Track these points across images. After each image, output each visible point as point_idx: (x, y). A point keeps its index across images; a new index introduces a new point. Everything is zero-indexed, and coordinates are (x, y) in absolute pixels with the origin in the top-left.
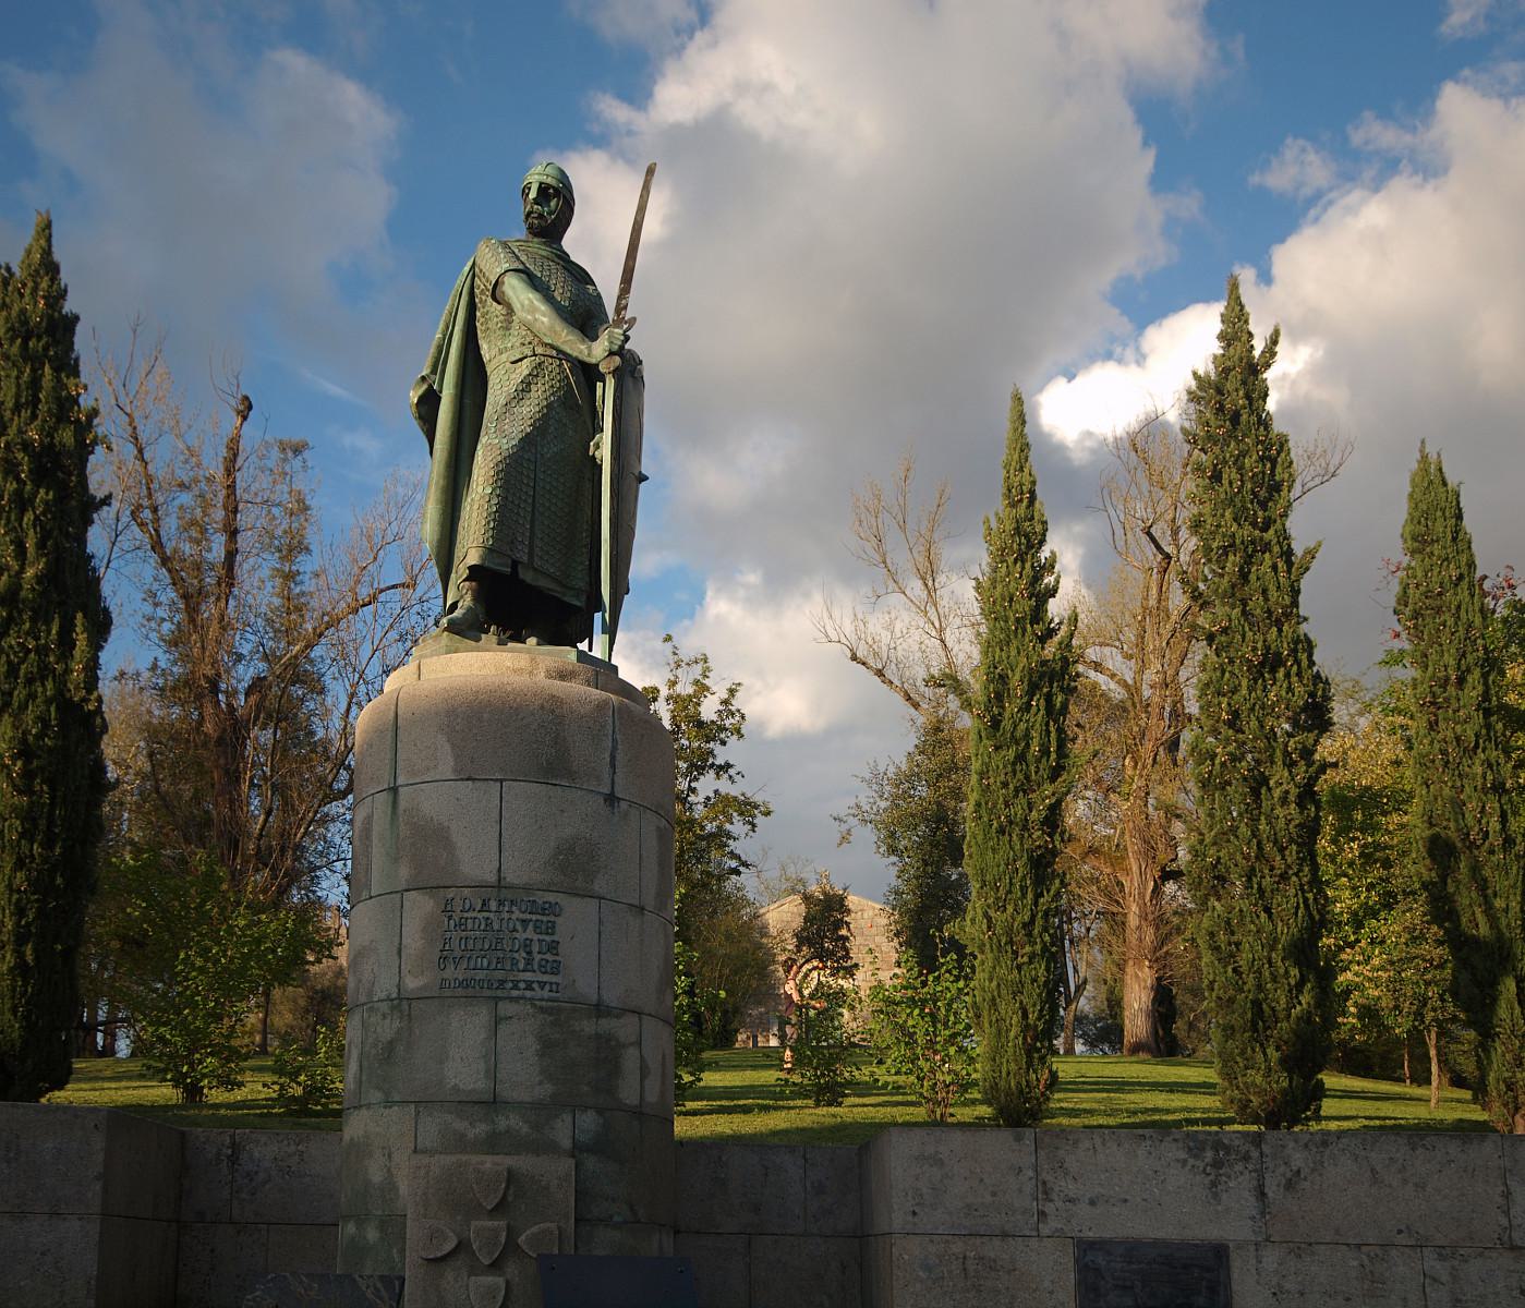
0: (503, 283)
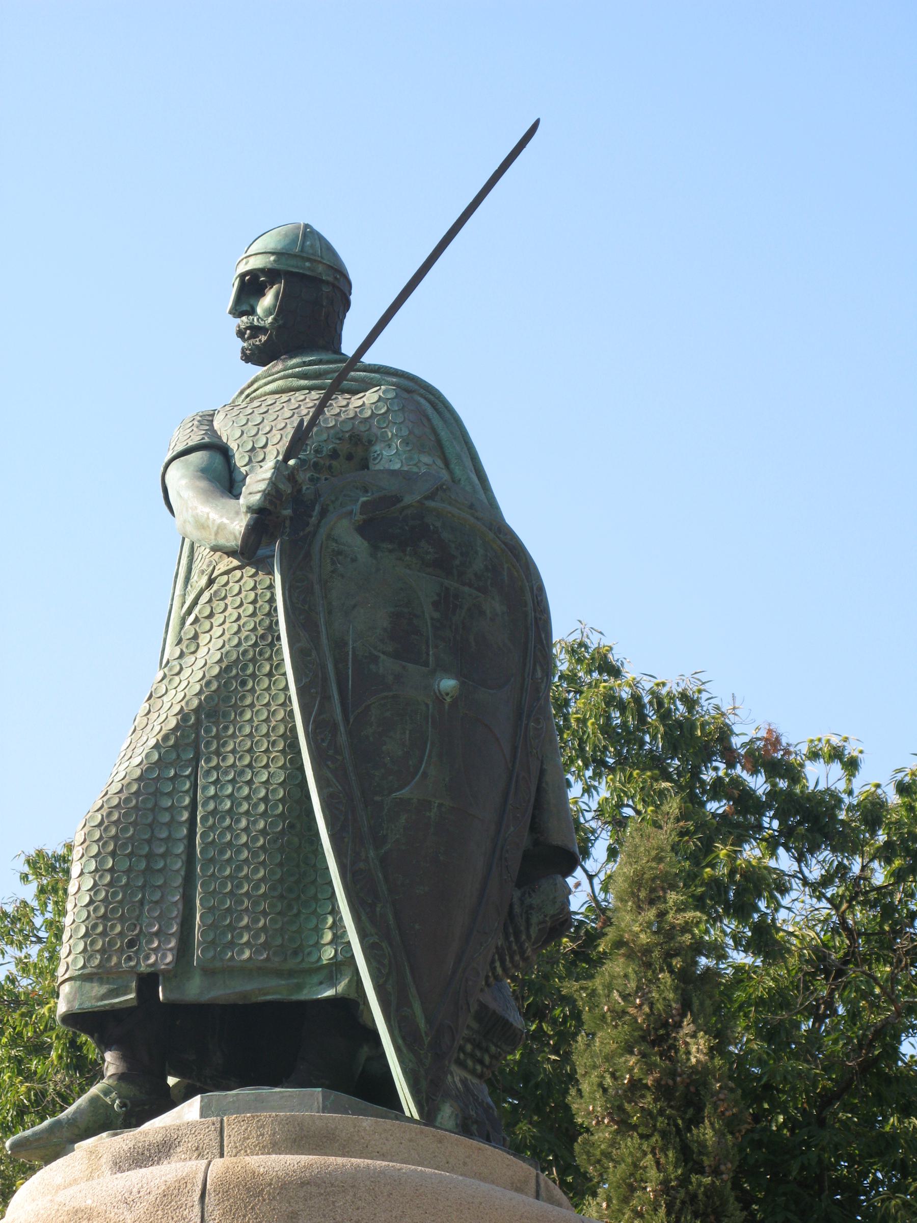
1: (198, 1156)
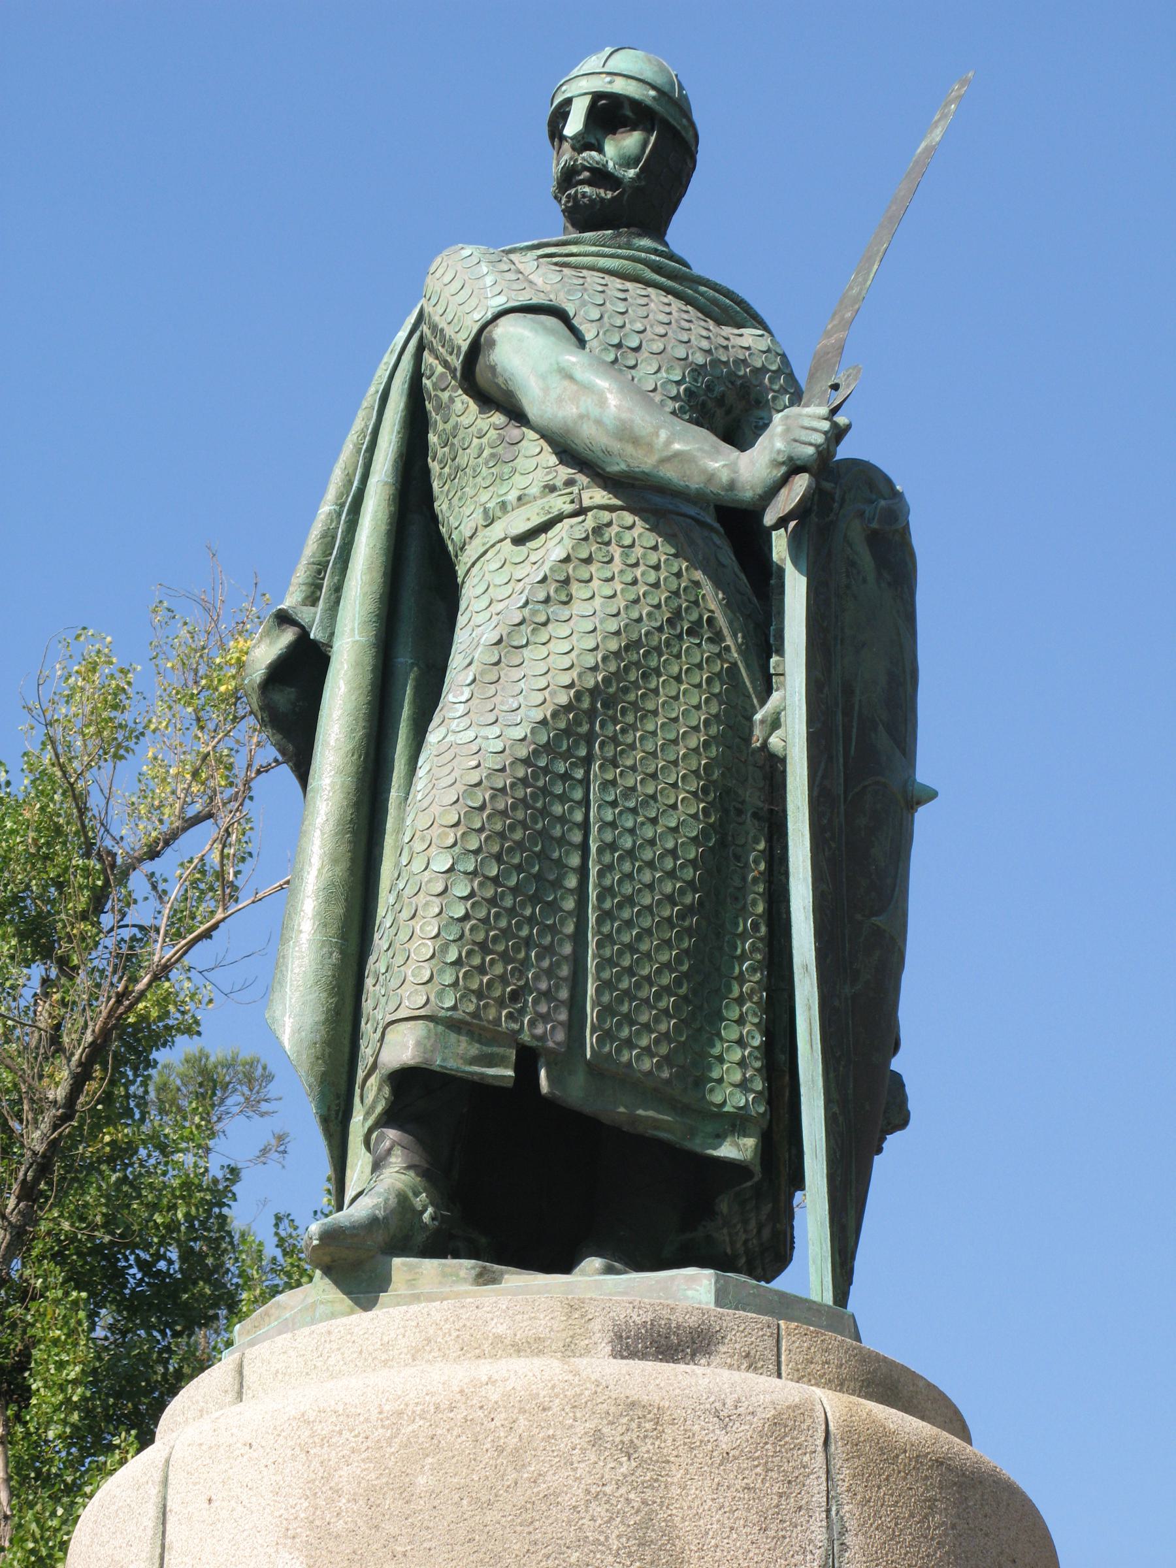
0: (492, 343)
1: (750, 1367)
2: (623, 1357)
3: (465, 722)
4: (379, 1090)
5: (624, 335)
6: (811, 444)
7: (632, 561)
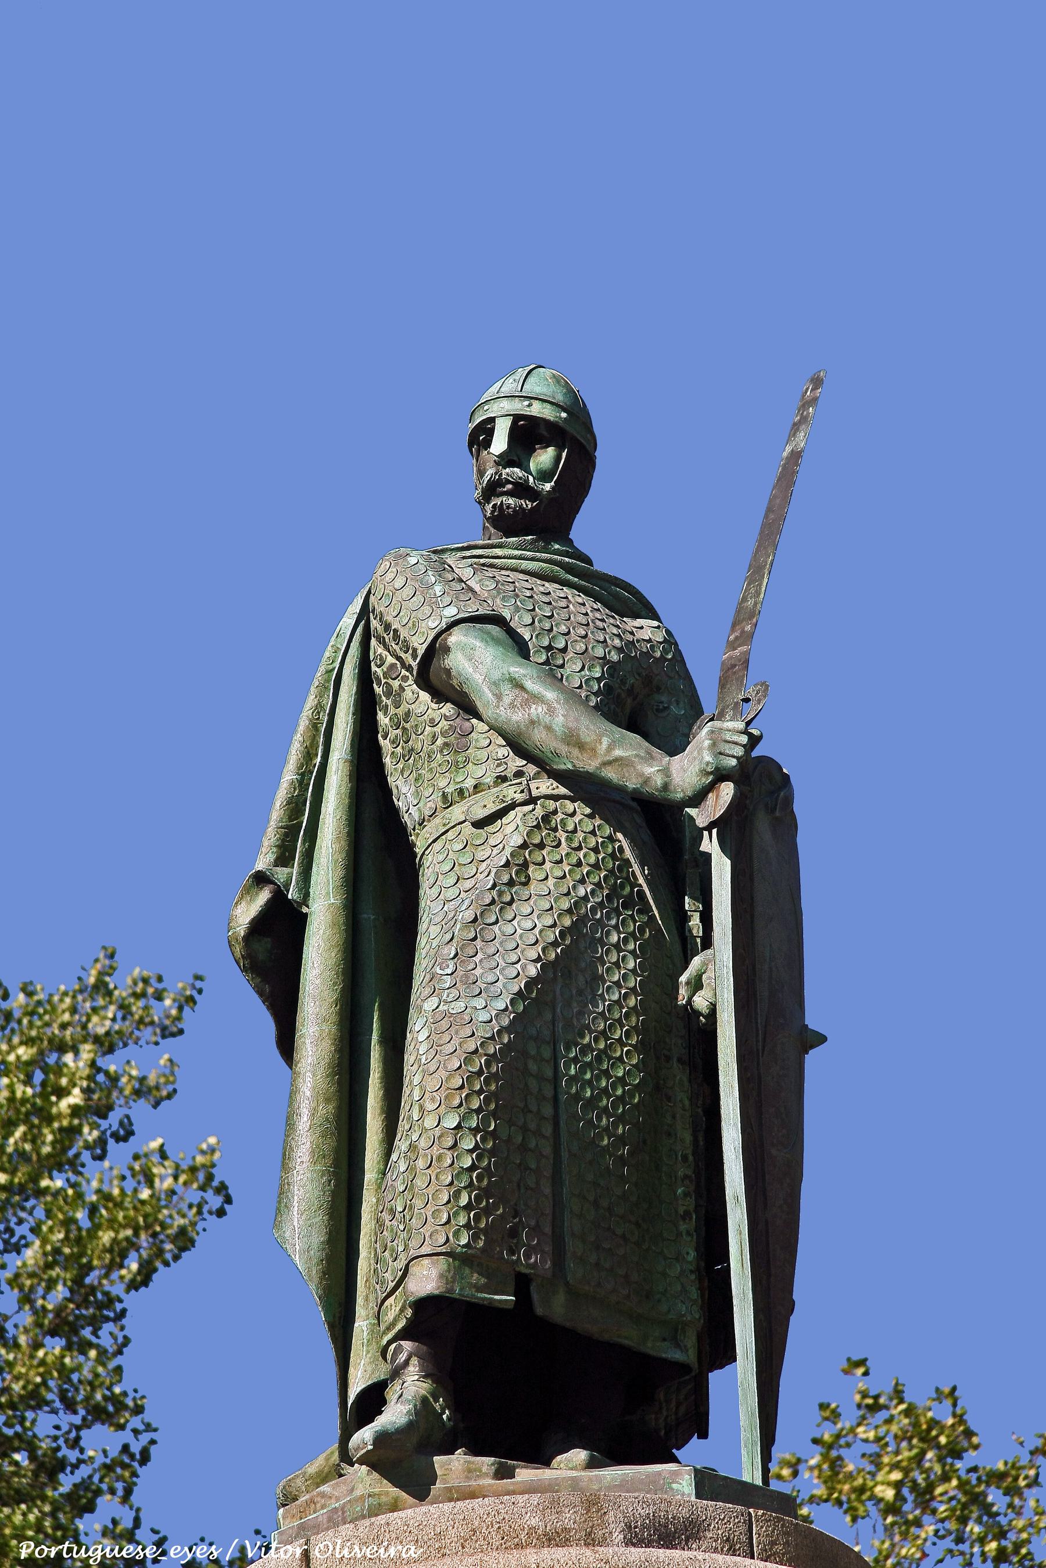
2: (634, 1545)
3: (454, 993)
4: (402, 1310)
5: (552, 637)
6: (733, 757)
7: (576, 844)
